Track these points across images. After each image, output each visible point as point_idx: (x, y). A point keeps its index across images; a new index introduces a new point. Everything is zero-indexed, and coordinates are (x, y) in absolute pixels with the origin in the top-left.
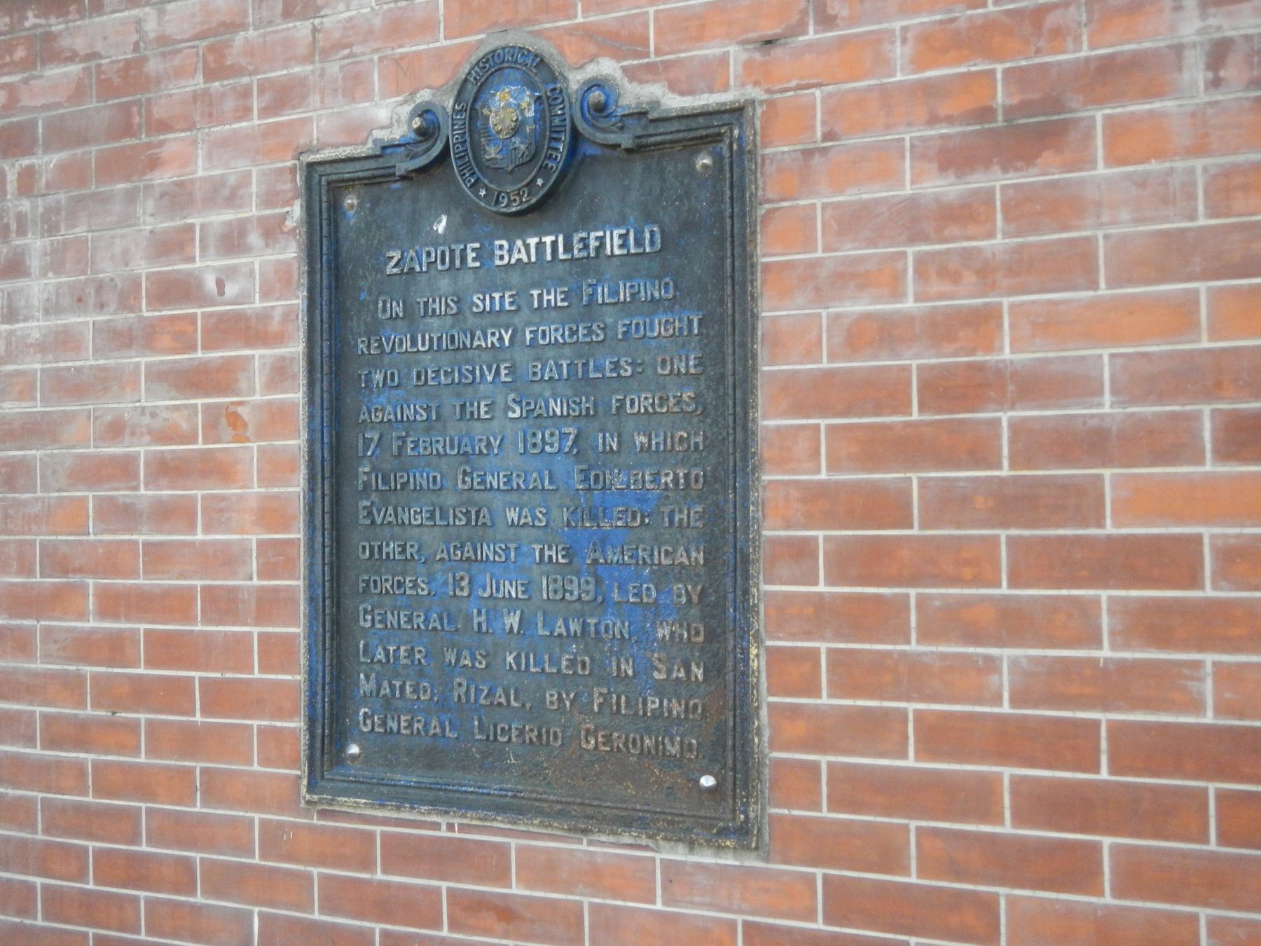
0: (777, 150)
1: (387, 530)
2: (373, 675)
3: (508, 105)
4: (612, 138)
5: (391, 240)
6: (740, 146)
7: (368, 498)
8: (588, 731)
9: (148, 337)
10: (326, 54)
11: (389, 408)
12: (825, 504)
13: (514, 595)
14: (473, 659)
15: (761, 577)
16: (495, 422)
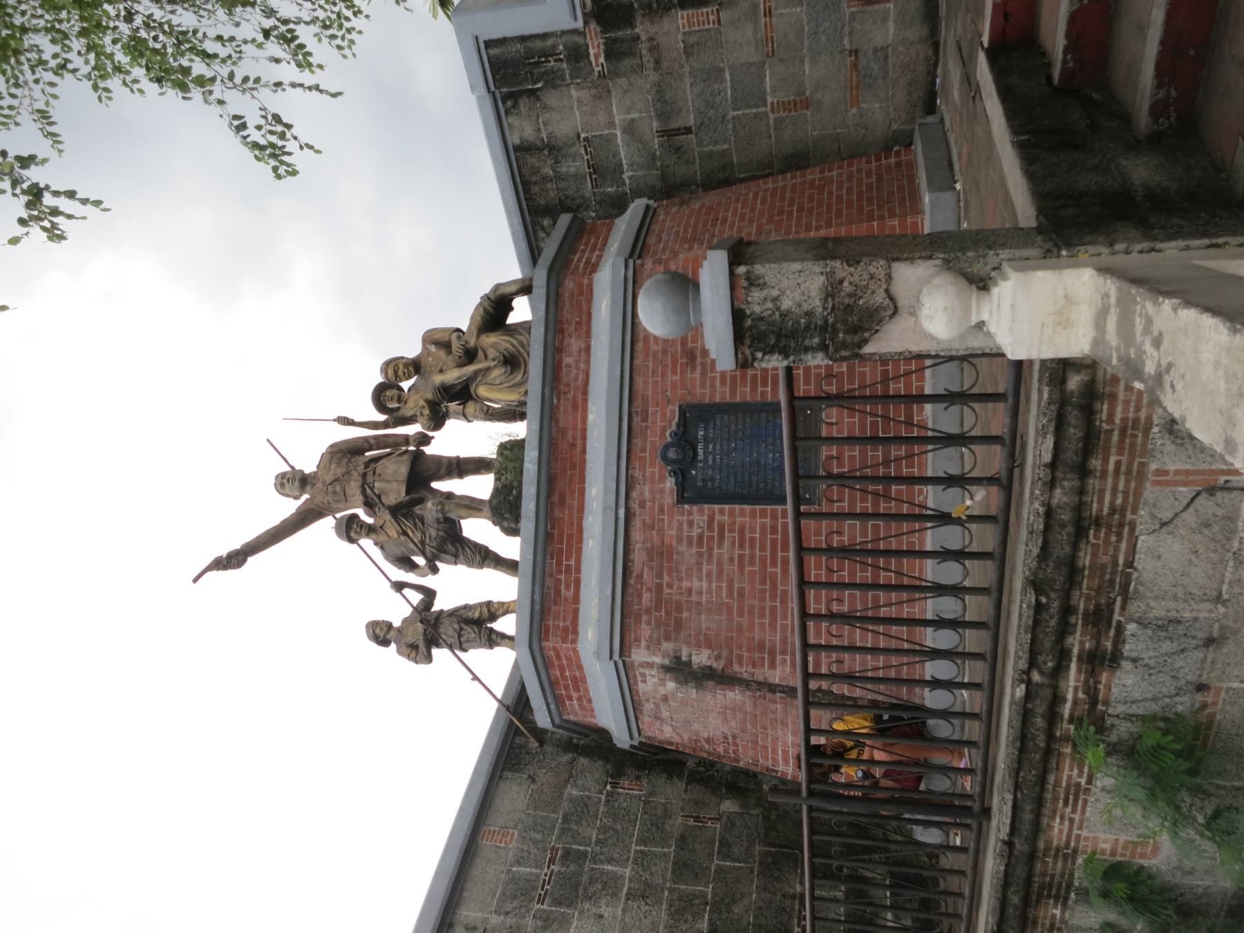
0: (688, 399)
3: (672, 454)
9: (710, 549)
10: (654, 498)
12: (754, 389)
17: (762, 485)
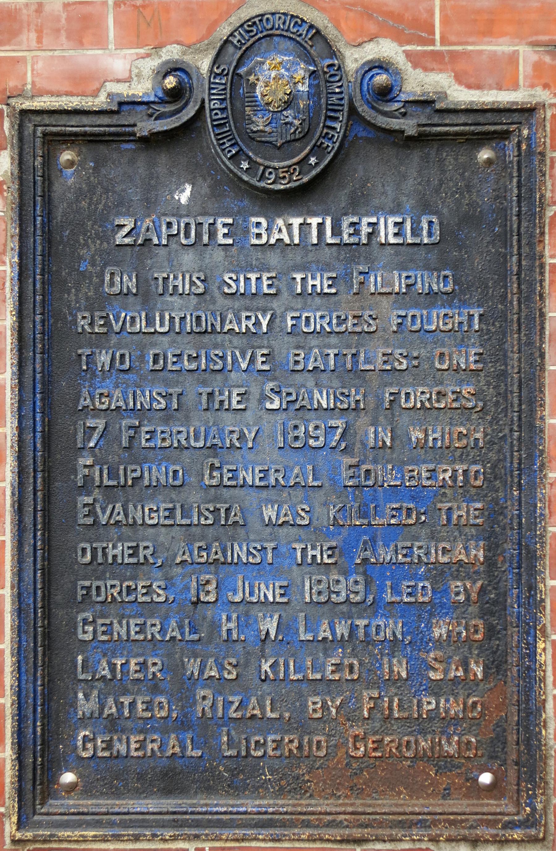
1: (114, 532)
2: (95, 693)
3: (277, 76)
4: (395, 124)
5: (122, 206)
6: (529, 146)
7: (88, 495)
8: (356, 737)
11: (117, 393)
13: (271, 599)
14: (221, 668)
15: (547, 572)
16: (248, 413)
17: (118, 550)
